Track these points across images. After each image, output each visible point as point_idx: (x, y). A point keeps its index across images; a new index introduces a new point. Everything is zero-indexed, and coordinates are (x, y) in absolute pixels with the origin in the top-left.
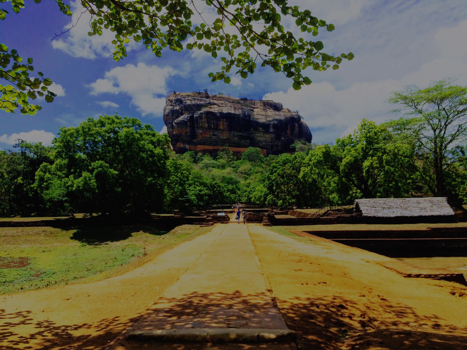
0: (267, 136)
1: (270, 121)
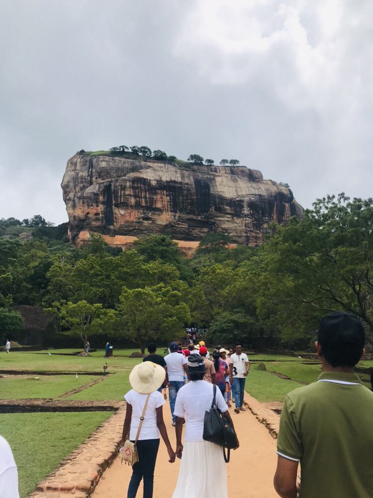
0: (238, 221)
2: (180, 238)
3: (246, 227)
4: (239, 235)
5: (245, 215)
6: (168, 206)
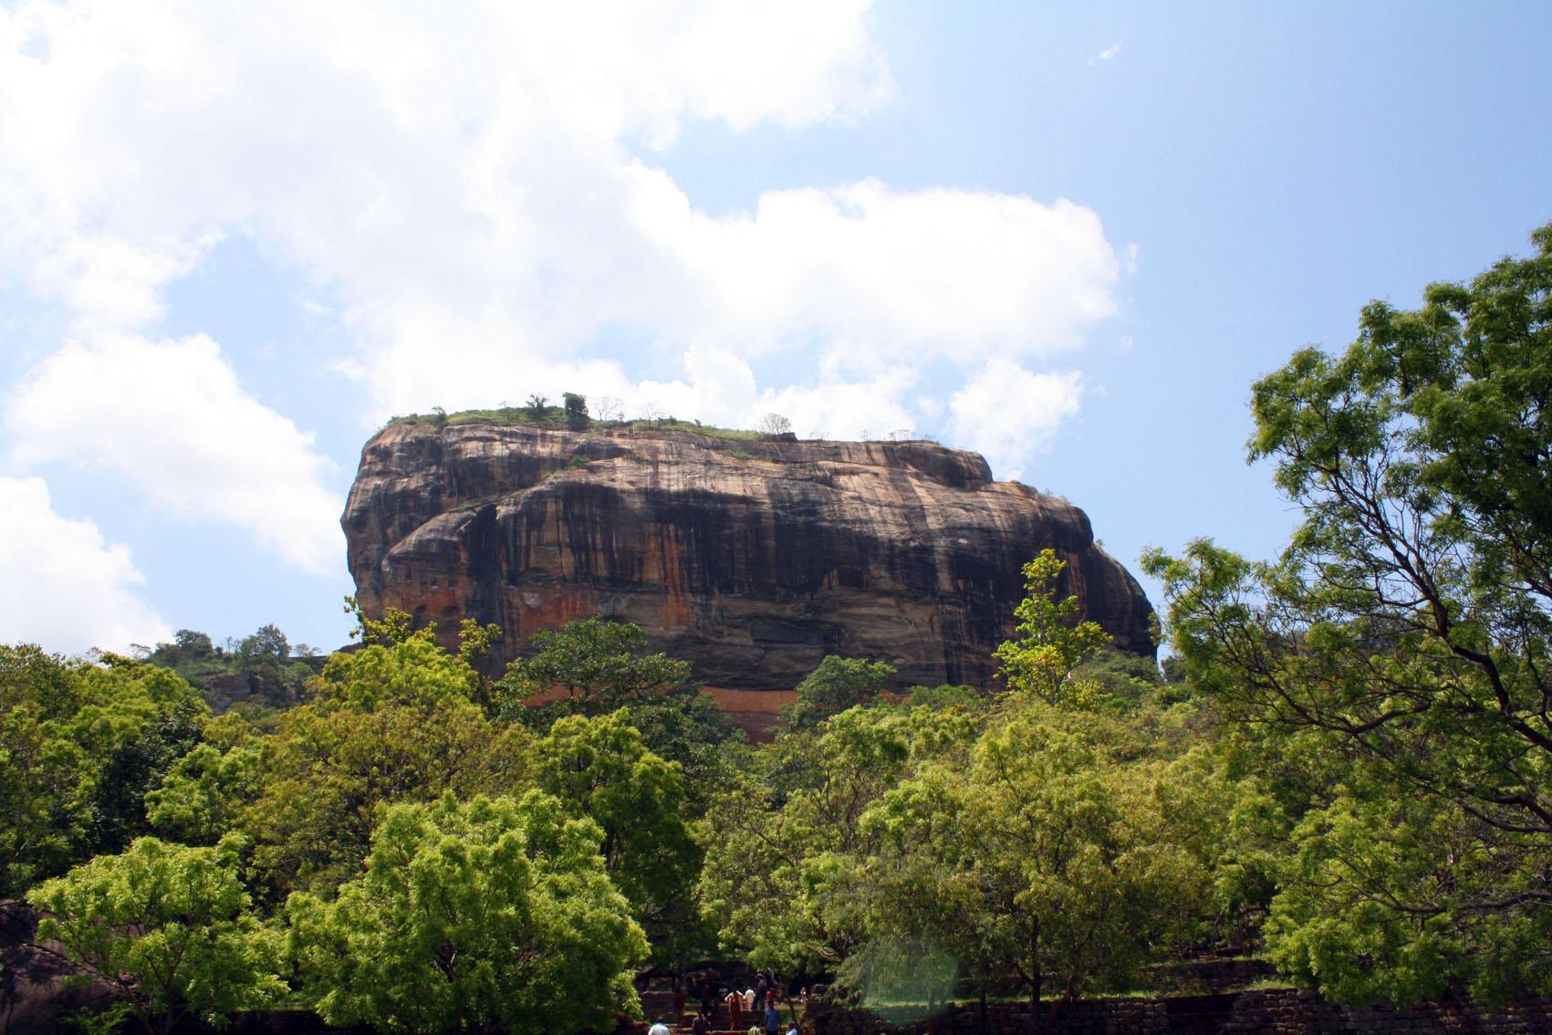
0: (920, 614)
1: (929, 535)
2: (726, 679)
3: (943, 633)
4: (924, 662)
5: (942, 597)
6: (681, 574)
